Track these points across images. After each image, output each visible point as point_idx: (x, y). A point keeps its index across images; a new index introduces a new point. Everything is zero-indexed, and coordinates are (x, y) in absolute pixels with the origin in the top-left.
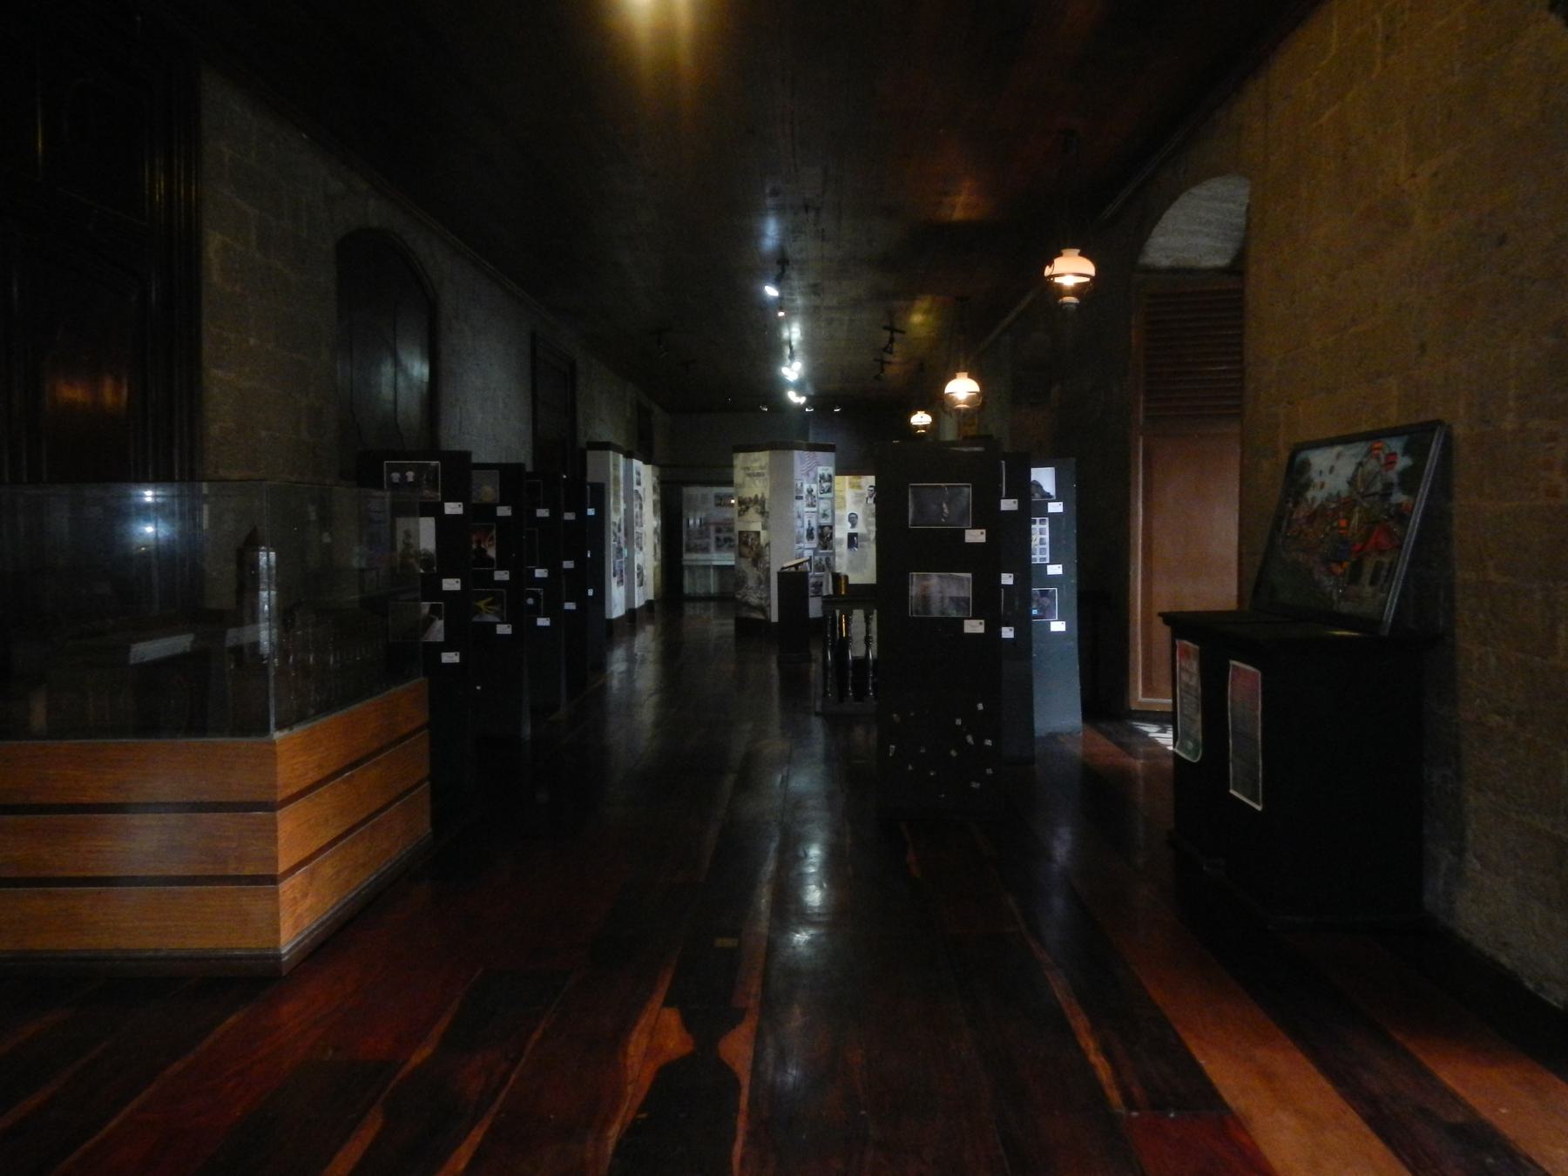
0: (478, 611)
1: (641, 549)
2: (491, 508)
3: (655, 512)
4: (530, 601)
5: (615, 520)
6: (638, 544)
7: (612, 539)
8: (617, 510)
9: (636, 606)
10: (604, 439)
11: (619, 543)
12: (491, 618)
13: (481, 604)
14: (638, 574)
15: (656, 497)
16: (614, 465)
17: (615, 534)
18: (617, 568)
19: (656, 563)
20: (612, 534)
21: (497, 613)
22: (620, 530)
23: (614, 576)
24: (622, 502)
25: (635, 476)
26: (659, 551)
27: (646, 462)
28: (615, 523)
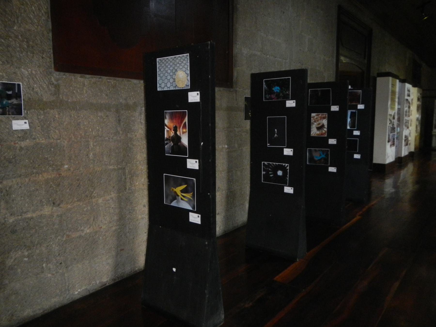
0: (175, 197)
1: (408, 128)
2: (184, 93)
3: (418, 110)
4: (280, 173)
5: (391, 113)
6: (406, 126)
7: (388, 123)
8: (393, 108)
9: (403, 155)
10: (387, 70)
11: (393, 125)
12: (185, 205)
13: (178, 190)
14: (405, 140)
15: (419, 103)
16: (392, 85)
17: (390, 120)
18: (390, 138)
19: (416, 134)
20: (388, 122)
21: (189, 201)
22: (394, 118)
23: (388, 142)
24: (396, 104)
25: (406, 92)
26: (419, 128)
27: (414, 86)
28: (391, 115)
